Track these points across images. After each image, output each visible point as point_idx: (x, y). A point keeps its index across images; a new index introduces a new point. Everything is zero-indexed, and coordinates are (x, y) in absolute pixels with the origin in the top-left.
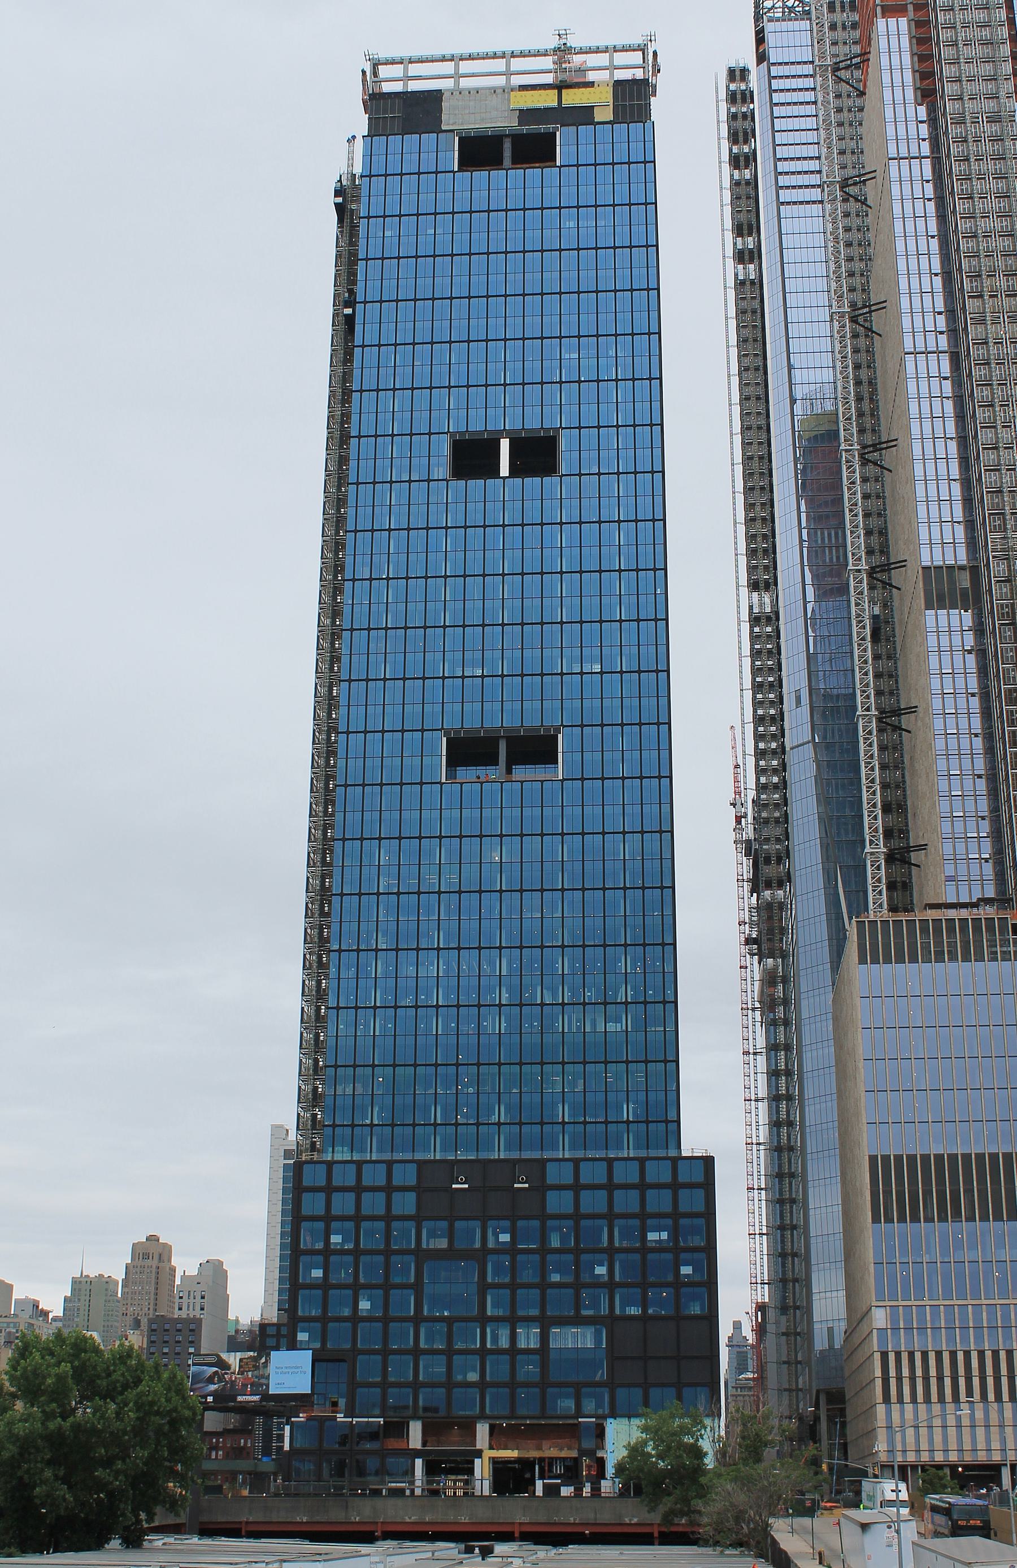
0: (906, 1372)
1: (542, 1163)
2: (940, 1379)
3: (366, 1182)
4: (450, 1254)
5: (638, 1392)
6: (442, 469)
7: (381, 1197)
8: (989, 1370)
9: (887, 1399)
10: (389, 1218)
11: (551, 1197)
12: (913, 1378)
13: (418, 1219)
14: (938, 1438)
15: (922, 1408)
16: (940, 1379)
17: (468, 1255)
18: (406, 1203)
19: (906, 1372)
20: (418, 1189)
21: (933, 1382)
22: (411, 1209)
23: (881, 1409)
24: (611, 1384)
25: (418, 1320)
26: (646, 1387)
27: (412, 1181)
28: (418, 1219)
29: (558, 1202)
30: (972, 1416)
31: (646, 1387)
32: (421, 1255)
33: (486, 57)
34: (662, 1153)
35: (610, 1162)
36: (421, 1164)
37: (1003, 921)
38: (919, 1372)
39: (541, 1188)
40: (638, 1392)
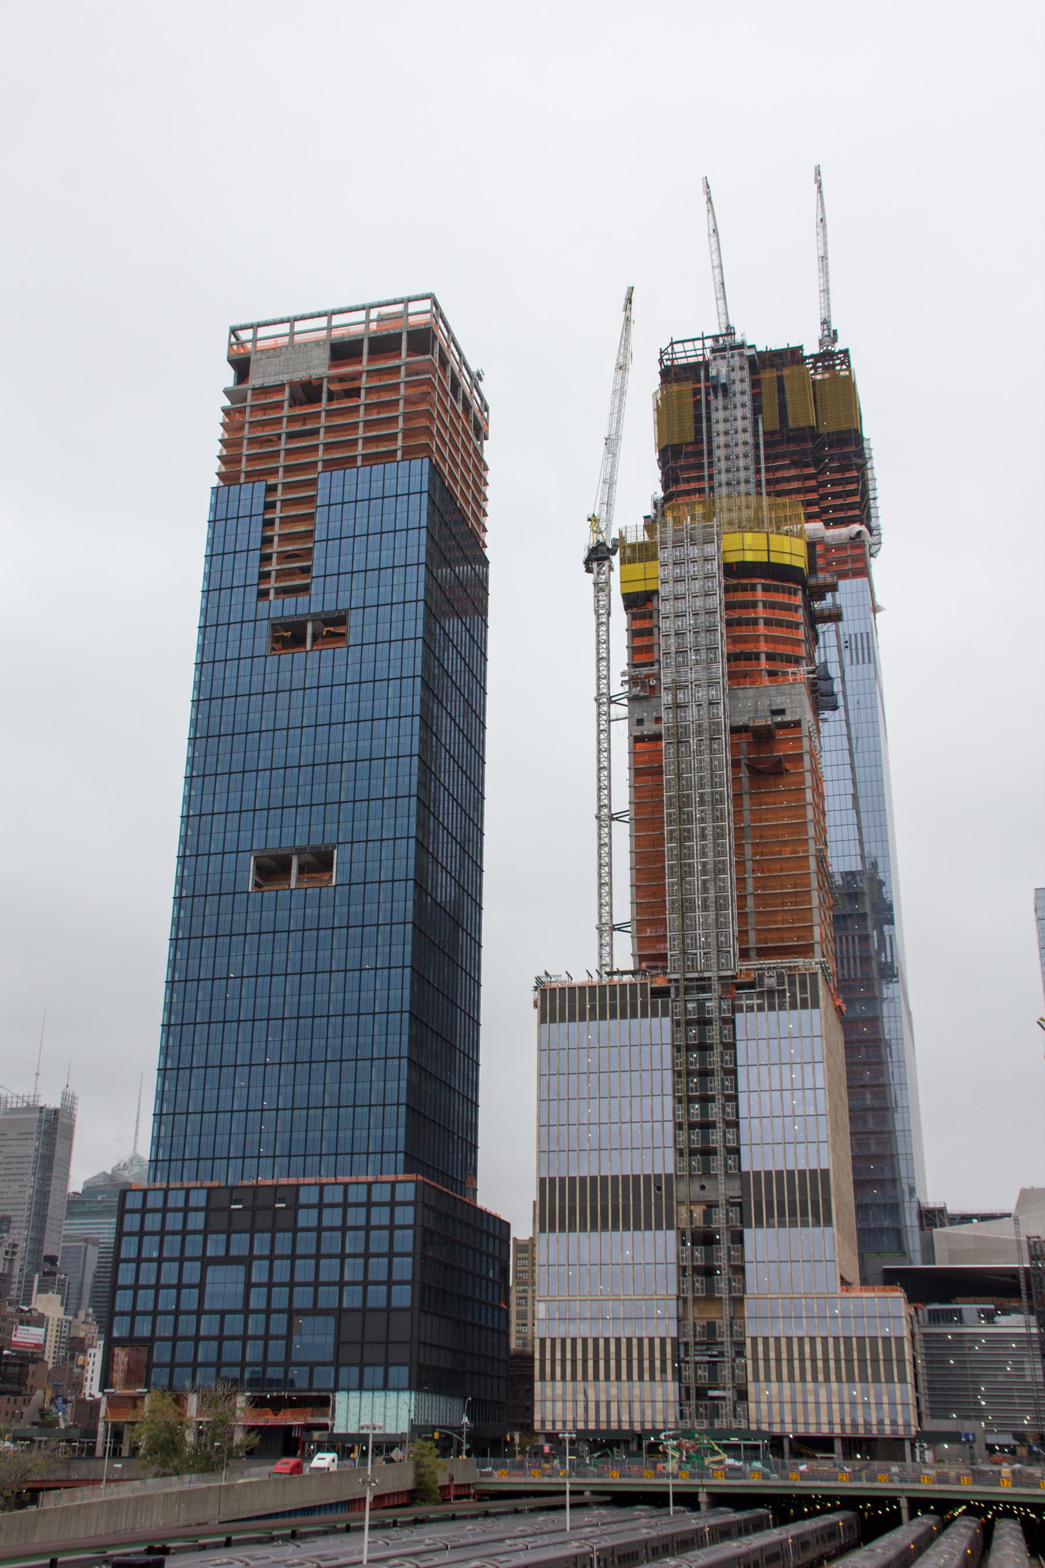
0: (558, 1355)
1: (297, 1187)
2: (585, 1361)
3: (327, 1200)
4: (227, 1260)
5: (355, 1371)
6: (263, 643)
7: (362, 1211)
8: (624, 1355)
9: (543, 1378)
10: (184, 1232)
11: (302, 1213)
12: (563, 1361)
13: (205, 1233)
14: (581, 1411)
15: (787, 1386)
16: (585, 1361)
17: (237, 1260)
18: (197, 1221)
19: (558, 1355)
20: (207, 1209)
21: (579, 1363)
22: (201, 1226)
23: (537, 1385)
24: (337, 1363)
25: (200, 1312)
26: (362, 1366)
27: (202, 1203)
28: (205, 1233)
29: (307, 1218)
30: (816, 1394)
31: (362, 1366)
32: (206, 1262)
33: (312, 317)
34: (362, 1178)
35: (322, 1186)
36: (210, 1190)
37: (644, 985)
38: (569, 1356)
39: (295, 1207)
40: (355, 1371)
